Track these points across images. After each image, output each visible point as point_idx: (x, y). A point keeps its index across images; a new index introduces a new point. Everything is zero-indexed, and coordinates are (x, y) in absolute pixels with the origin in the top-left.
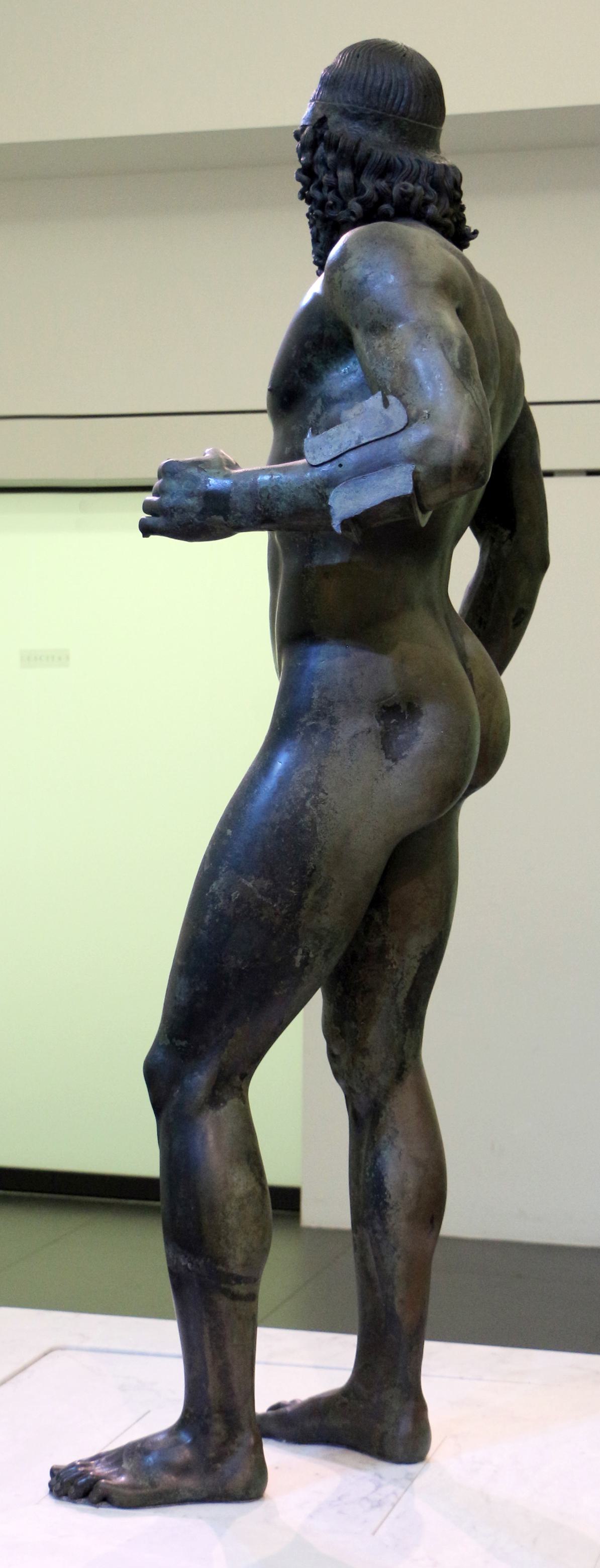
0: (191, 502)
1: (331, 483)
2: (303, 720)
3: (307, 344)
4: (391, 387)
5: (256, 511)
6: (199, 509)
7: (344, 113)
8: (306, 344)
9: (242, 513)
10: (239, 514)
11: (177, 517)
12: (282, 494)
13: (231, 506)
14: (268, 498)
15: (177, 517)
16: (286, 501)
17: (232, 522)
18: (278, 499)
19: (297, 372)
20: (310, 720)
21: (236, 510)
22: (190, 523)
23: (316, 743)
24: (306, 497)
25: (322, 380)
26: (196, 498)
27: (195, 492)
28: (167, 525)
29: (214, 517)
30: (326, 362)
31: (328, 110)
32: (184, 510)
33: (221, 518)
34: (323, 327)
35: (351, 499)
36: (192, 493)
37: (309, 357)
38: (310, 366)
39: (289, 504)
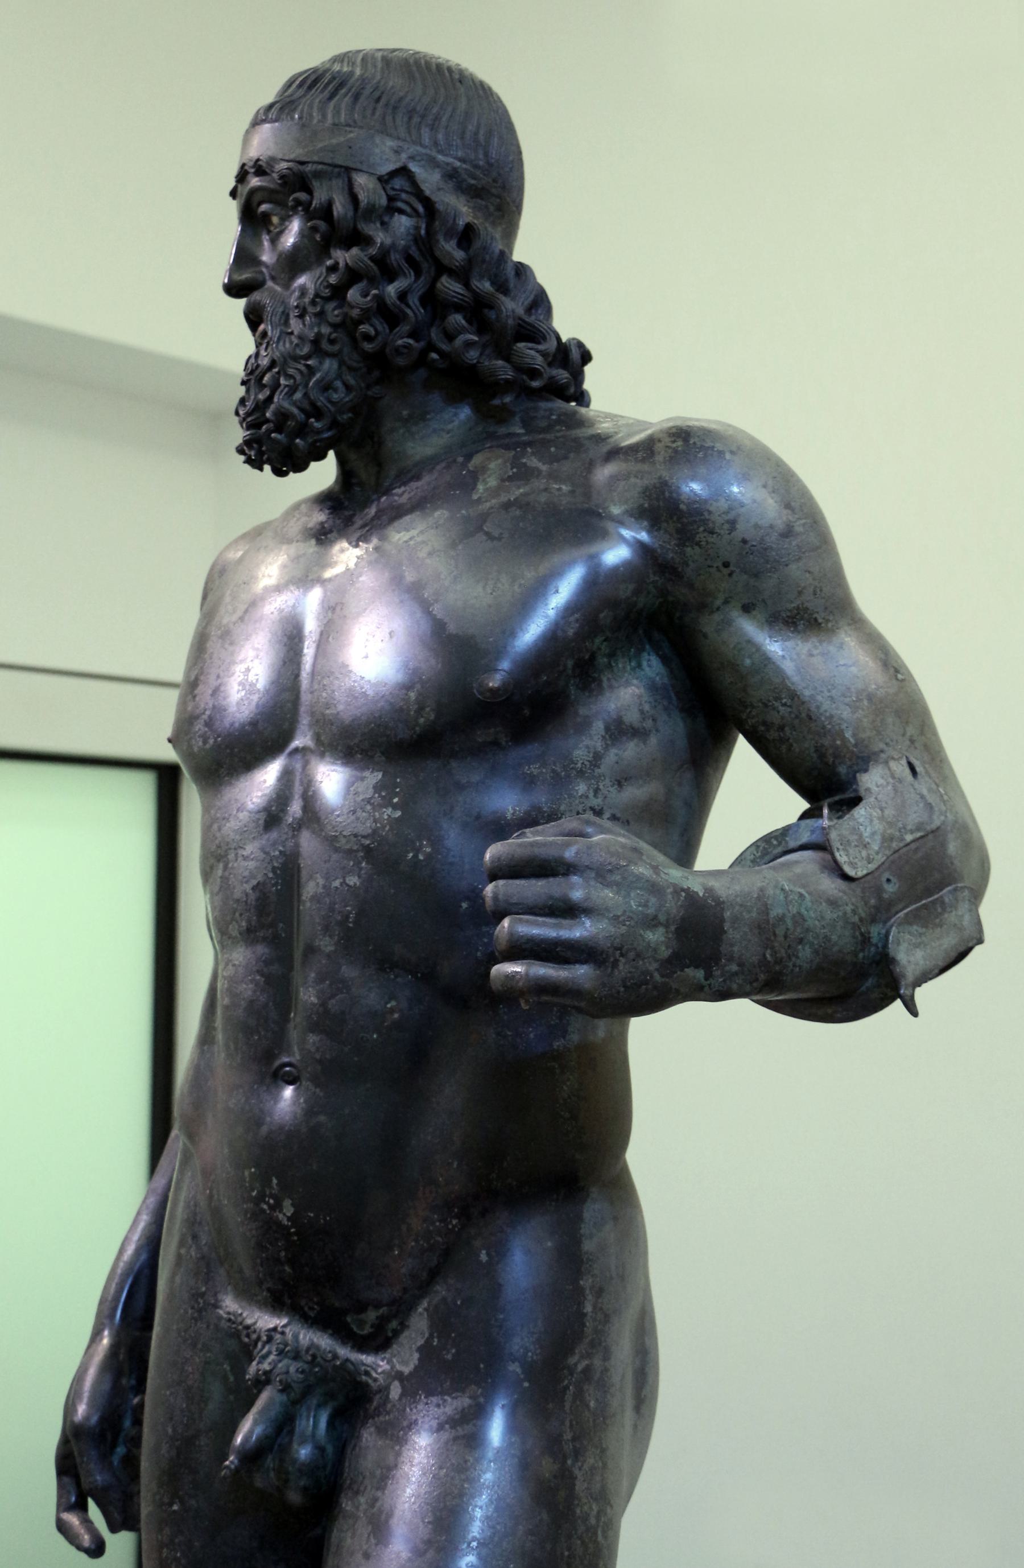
0: (654, 937)
1: (882, 911)
2: (572, 1360)
3: (605, 616)
4: (854, 735)
5: (763, 962)
6: (665, 953)
7: (451, 175)
8: (602, 615)
9: (741, 965)
10: (734, 968)
11: (623, 968)
12: (808, 930)
13: (724, 949)
14: (786, 937)
15: (623, 968)
16: (812, 944)
17: (717, 981)
18: (801, 941)
19: (570, 663)
20: (582, 1357)
21: (731, 959)
22: (647, 983)
23: (592, 1404)
24: (842, 940)
25: (601, 689)
26: (661, 930)
27: (662, 918)
28: (604, 985)
29: (690, 972)
30: (612, 655)
31: (412, 158)
32: (639, 955)
33: (700, 974)
34: (637, 592)
35: (917, 946)
36: (655, 917)
37: (598, 641)
38: (593, 657)
39: (816, 952)
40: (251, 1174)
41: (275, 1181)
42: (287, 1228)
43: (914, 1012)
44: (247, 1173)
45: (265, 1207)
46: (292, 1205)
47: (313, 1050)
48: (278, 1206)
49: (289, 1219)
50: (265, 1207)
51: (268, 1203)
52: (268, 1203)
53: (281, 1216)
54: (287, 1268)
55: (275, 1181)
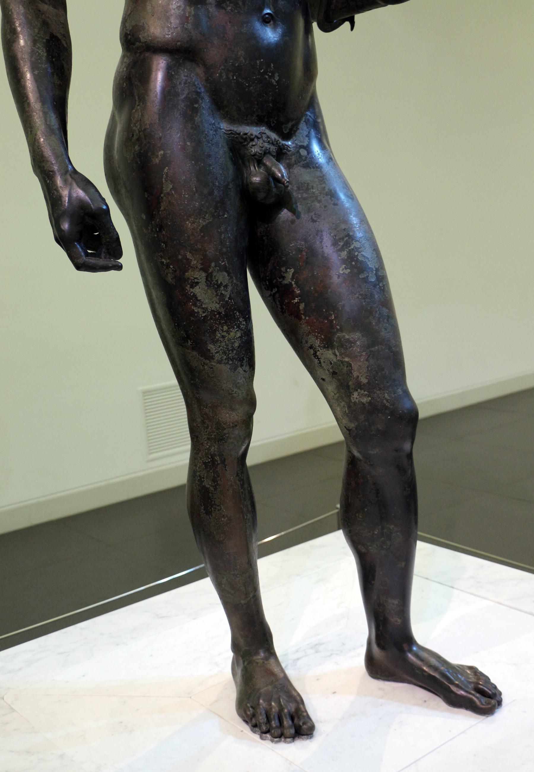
40: (260, 62)
41: (272, 65)
42: (275, 86)
43: (352, 29)
44: (258, 62)
45: (267, 77)
46: (278, 76)
47: (281, 7)
48: (273, 76)
49: (276, 82)
50: (267, 77)
51: (268, 75)
52: (268, 75)
53: (273, 81)
54: (271, 105)
55: (272, 65)
